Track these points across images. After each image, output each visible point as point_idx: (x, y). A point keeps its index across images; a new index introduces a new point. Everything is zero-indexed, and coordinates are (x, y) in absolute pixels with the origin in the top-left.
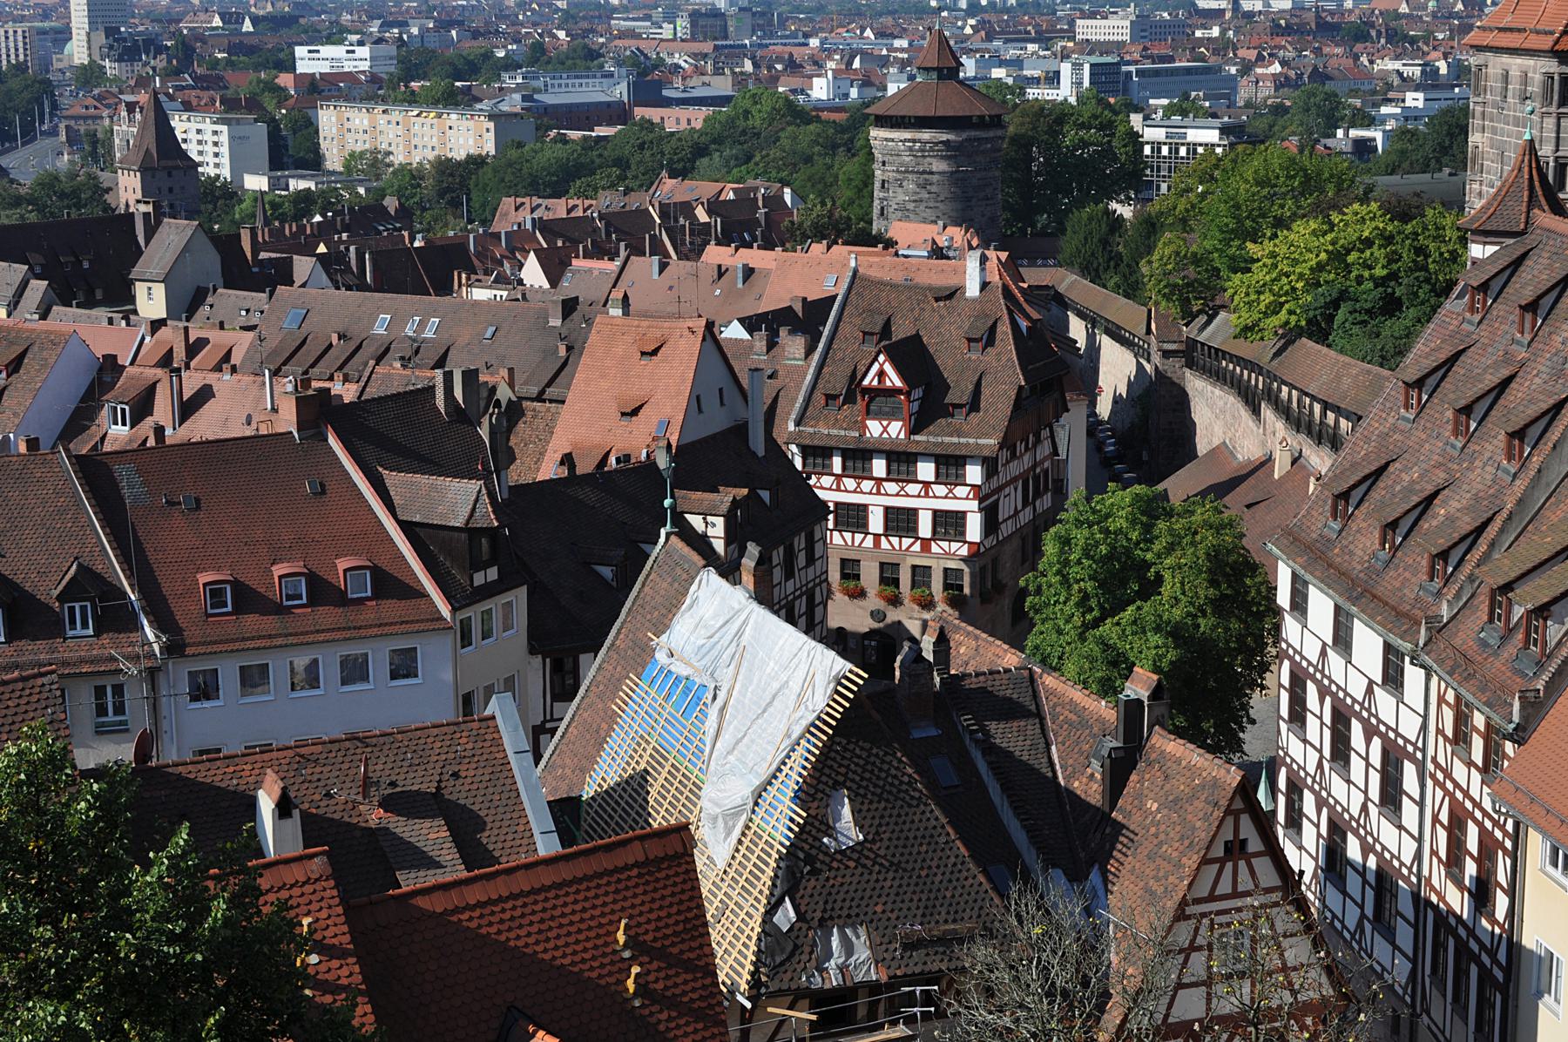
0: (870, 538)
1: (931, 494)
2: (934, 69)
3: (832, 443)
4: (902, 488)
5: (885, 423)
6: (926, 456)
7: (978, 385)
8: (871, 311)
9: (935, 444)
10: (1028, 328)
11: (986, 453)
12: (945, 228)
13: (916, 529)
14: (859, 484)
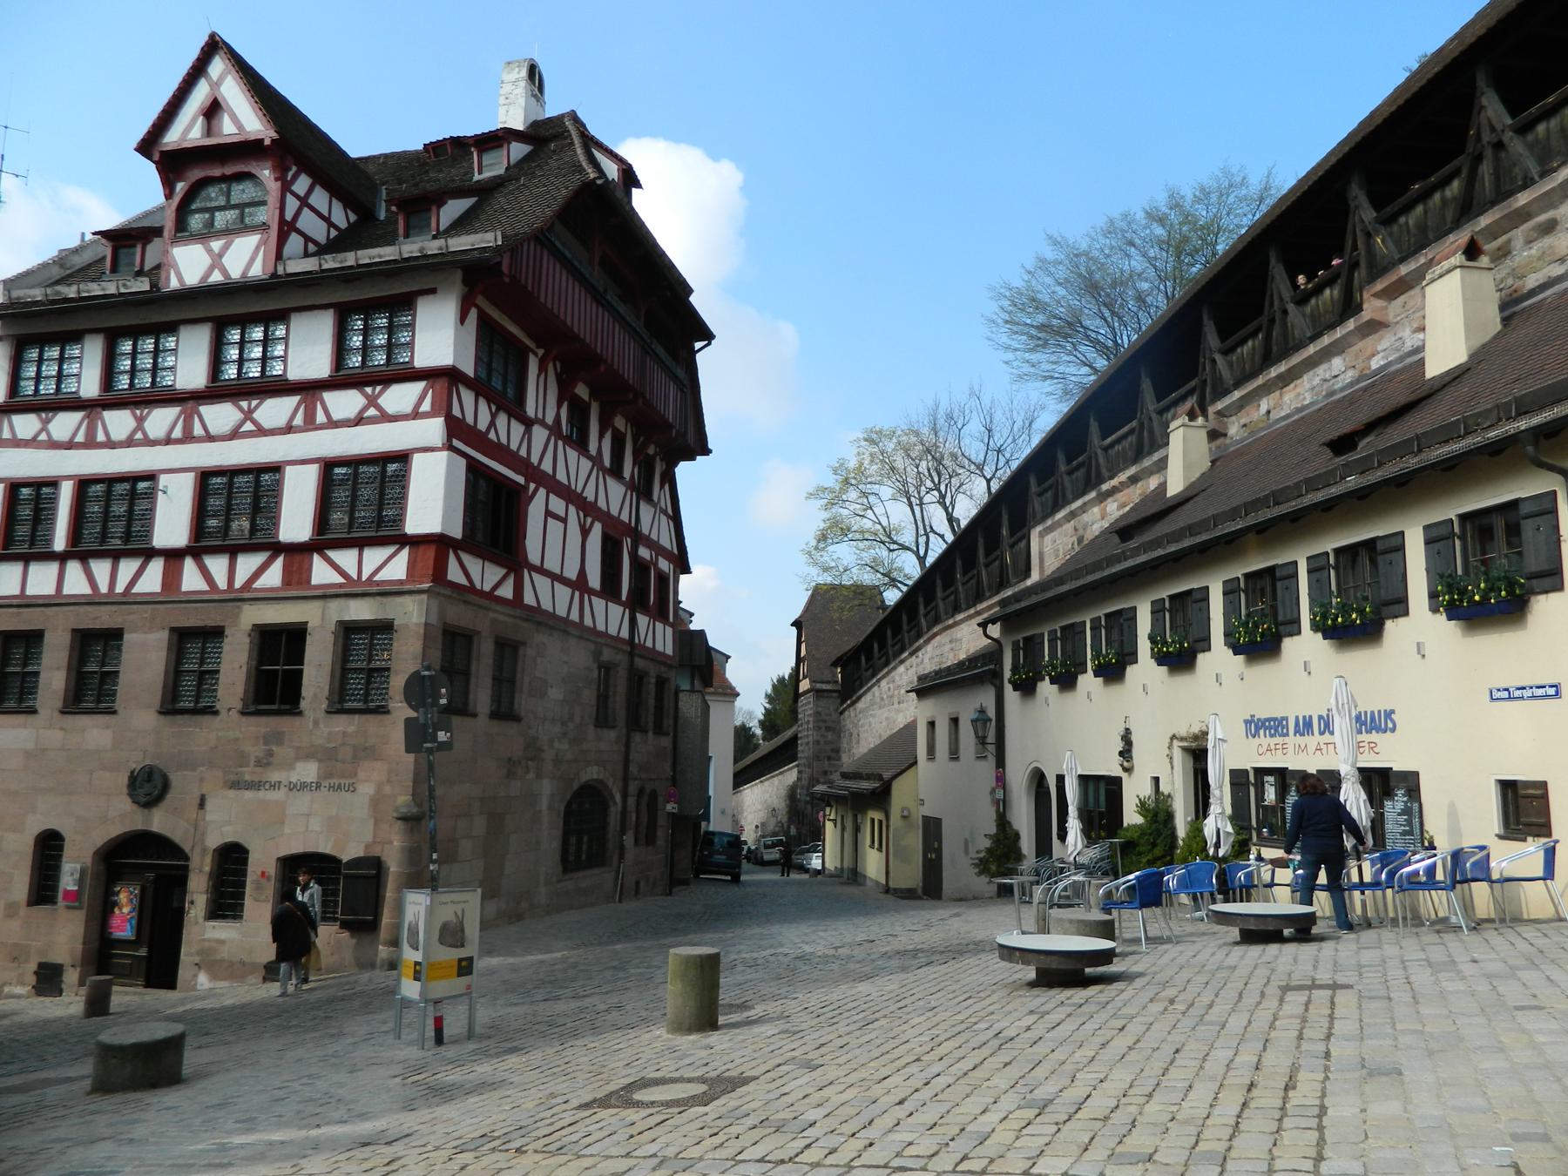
1: (321, 418)
4: (248, 415)
14: (140, 421)
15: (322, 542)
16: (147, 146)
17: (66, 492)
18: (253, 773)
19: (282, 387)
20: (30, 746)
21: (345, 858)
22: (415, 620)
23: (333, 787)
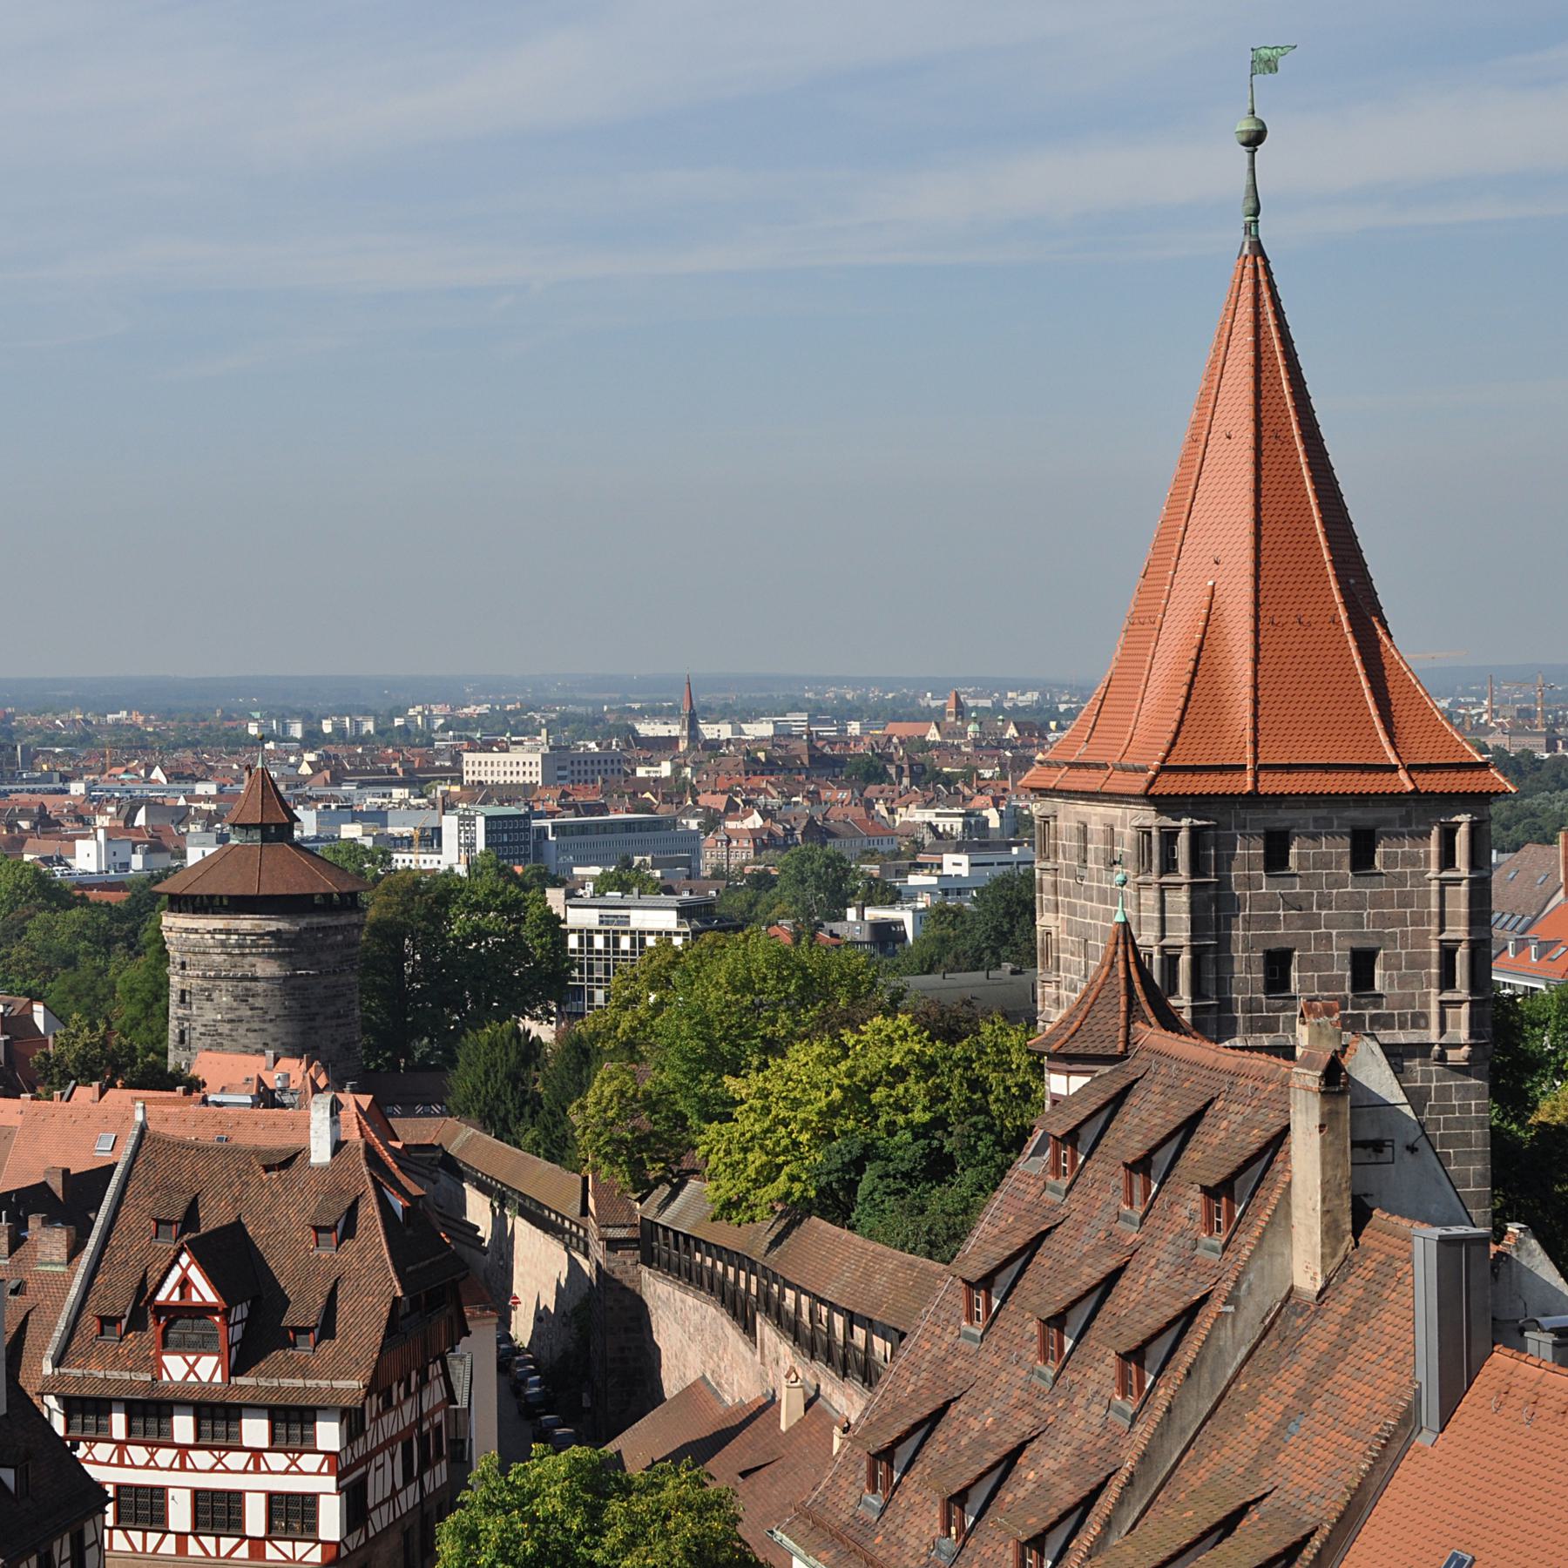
0: (171, 1538)
1: (264, 1468)
2: (255, 826)
3: (111, 1393)
4: (220, 1460)
5: (191, 1359)
6: (255, 1408)
7: (332, 1297)
8: (167, 1188)
9: (268, 1390)
10: (405, 1209)
11: (346, 1402)
12: (276, 1061)
13: (240, 1524)
14: (152, 1455)
15: (272, 1533)
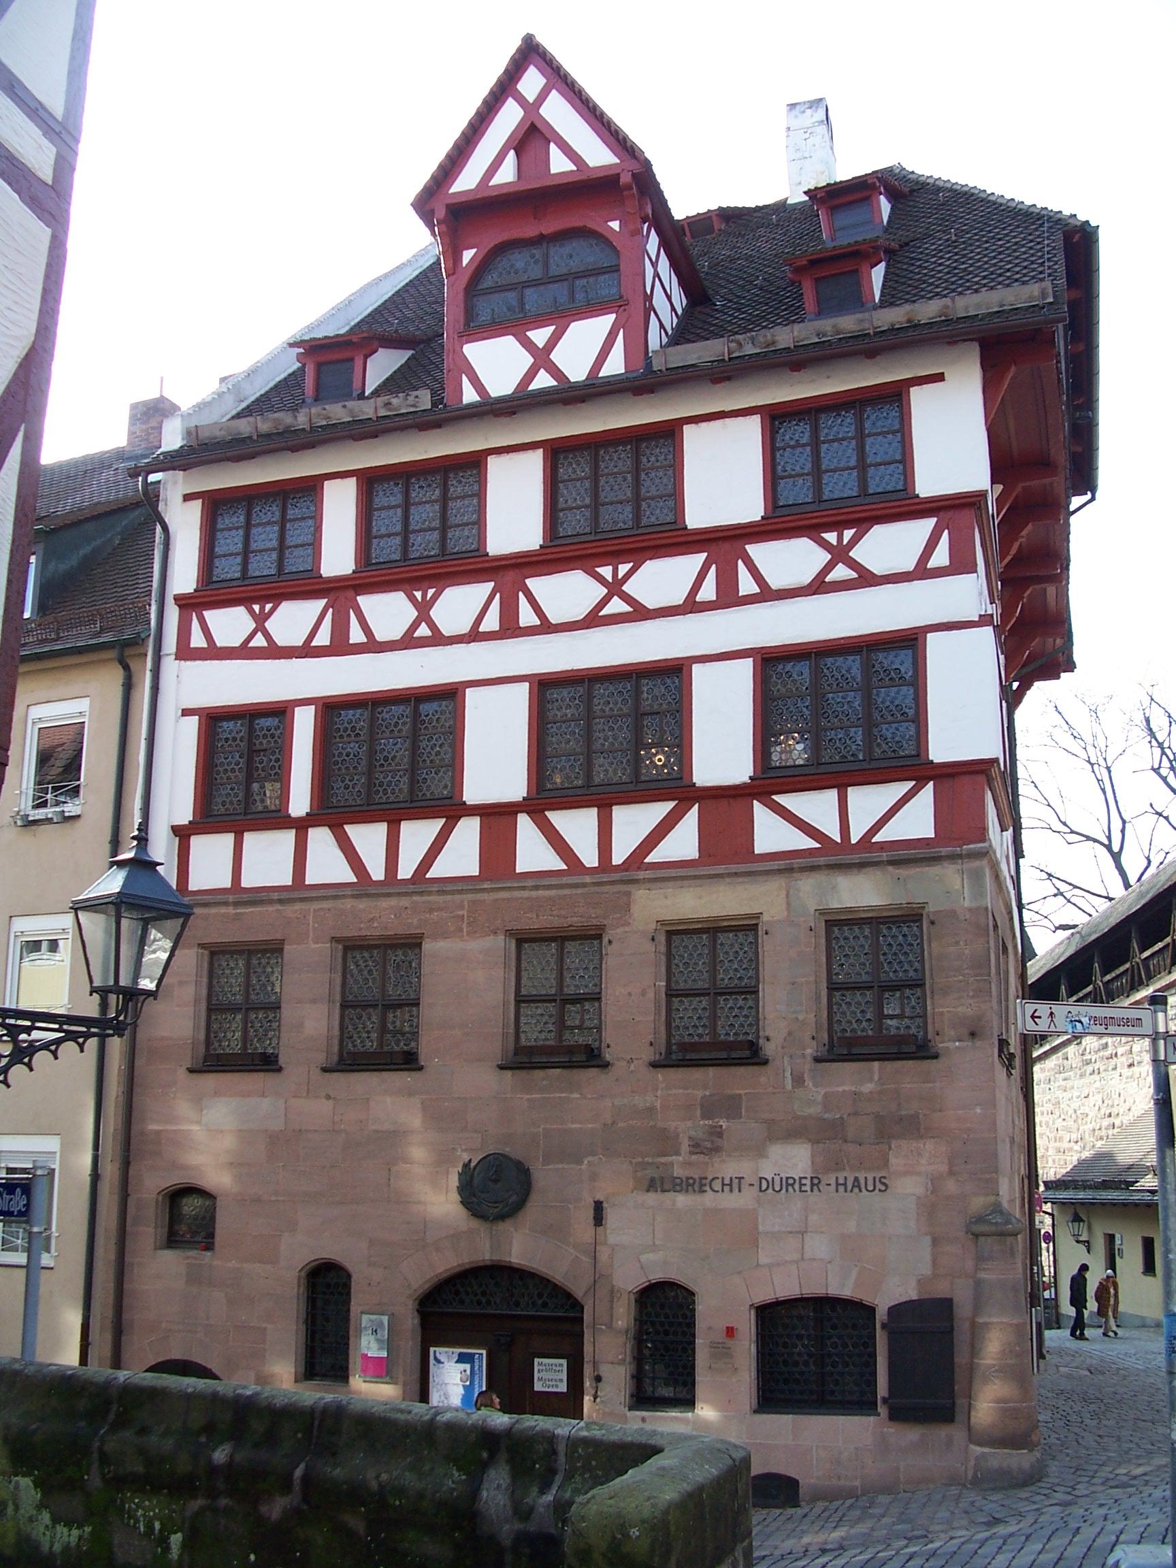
1: (747, 585)
4: (615, 588)
5: (540, 336)
16: (425, 204)
17: (304, 724)
18: (687, 1164)
19: (683, 540)
20: (277, 1125)
21: (883, 1303)
22: (967, 904)
23: (845, 1184)
